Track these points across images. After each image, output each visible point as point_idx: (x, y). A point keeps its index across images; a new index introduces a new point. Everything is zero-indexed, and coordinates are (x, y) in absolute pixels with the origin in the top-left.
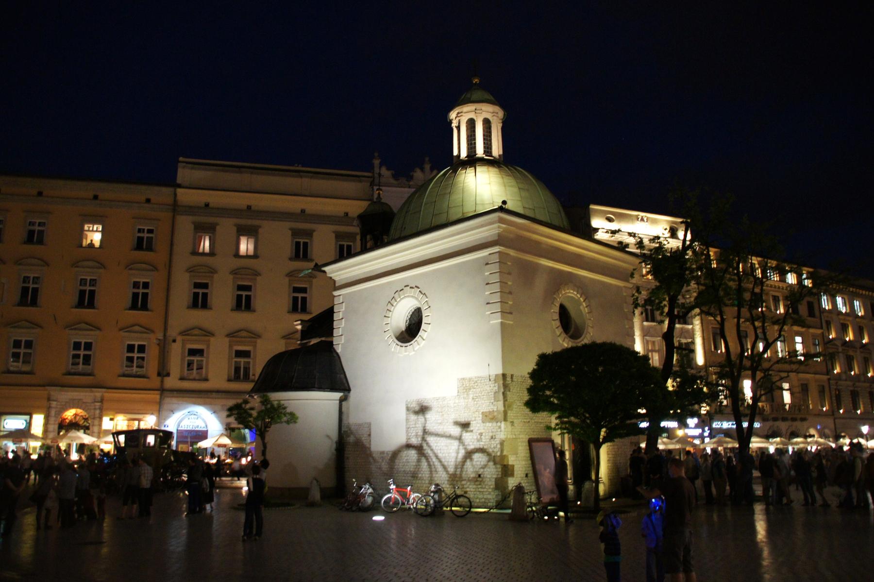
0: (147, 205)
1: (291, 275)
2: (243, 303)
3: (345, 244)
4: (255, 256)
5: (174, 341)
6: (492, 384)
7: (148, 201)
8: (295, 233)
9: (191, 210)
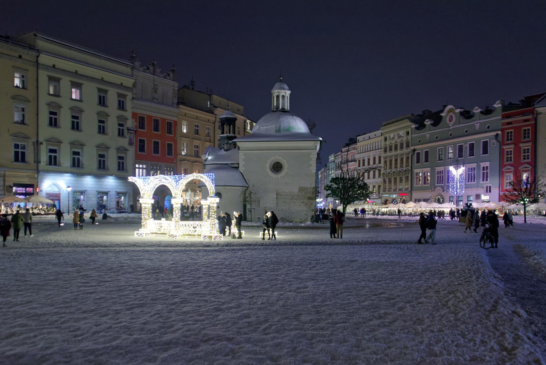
0: (19, 59)
1: (99, 114)
2: (76, 127)
3: (121, 100)
4: (81, 101)
5: (41, 144)
6: (311, 190)
7: (20, 57)
8: (100, 90)
9: (46, 67)
